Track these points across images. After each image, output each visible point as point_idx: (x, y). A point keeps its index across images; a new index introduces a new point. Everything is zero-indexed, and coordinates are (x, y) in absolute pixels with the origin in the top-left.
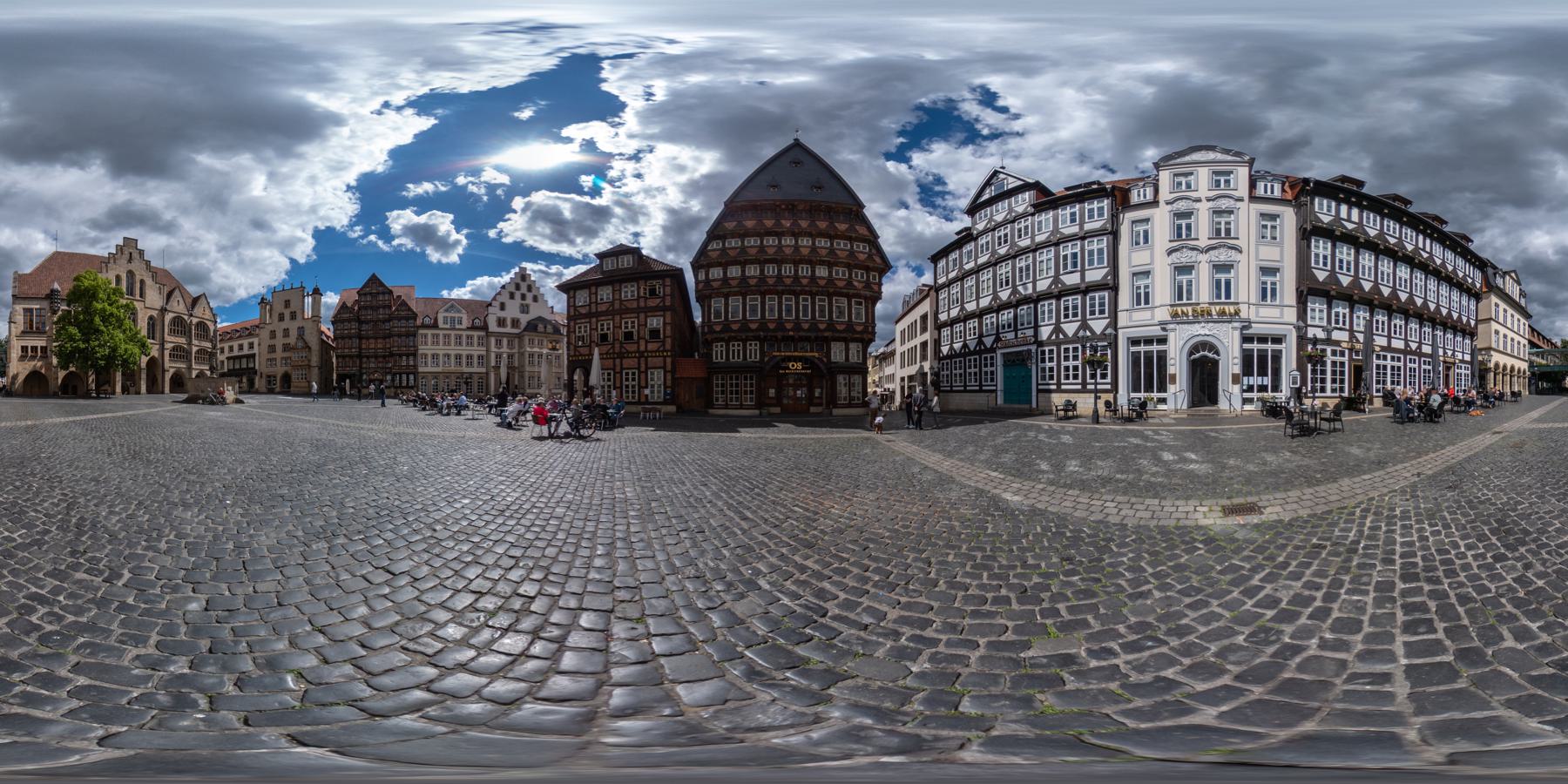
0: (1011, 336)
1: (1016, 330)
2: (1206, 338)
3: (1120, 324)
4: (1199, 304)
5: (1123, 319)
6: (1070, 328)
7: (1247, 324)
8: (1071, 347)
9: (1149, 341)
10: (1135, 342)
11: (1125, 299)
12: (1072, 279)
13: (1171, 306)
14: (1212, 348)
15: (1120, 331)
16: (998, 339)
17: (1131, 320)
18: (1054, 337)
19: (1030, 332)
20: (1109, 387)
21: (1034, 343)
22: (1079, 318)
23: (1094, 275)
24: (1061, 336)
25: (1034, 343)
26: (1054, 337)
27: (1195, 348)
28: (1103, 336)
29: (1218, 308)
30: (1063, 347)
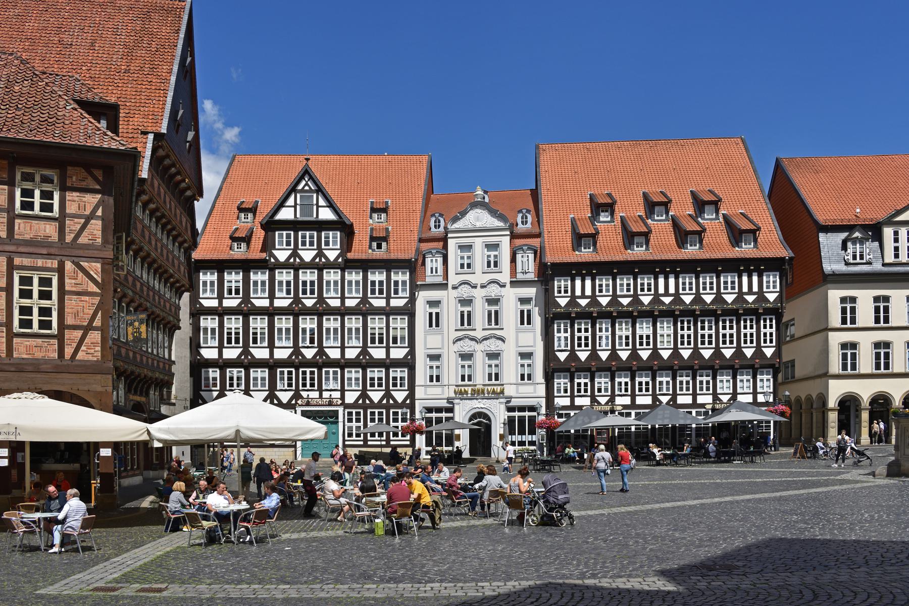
0: (315, 395)
1: (320, 390)
2: (484, 411)
3: (417, 396)
4: (475, 385)
5: (419, 393)
6: (376, 396)
7: (508, 400)
8: (377, 411)
9: (439, 410)
10: (429, 410)
11: (421, 377)
12: (378, 353)
13: (457, 386)
14: (486, 416)
15: (417, 402)
16: (297, 396)
17: (425, 394)
18: (360, 402)
19: (337, 395)
20: (408, 443)
21: (341, 404)
22: (384, 388)
23: (398, 353)
24: (368, 402)
25: (341, 404)
26: (360, 402)
27: (473, 417)
28: (402, 405)
29: (489, 388)
30: (369, 411)
